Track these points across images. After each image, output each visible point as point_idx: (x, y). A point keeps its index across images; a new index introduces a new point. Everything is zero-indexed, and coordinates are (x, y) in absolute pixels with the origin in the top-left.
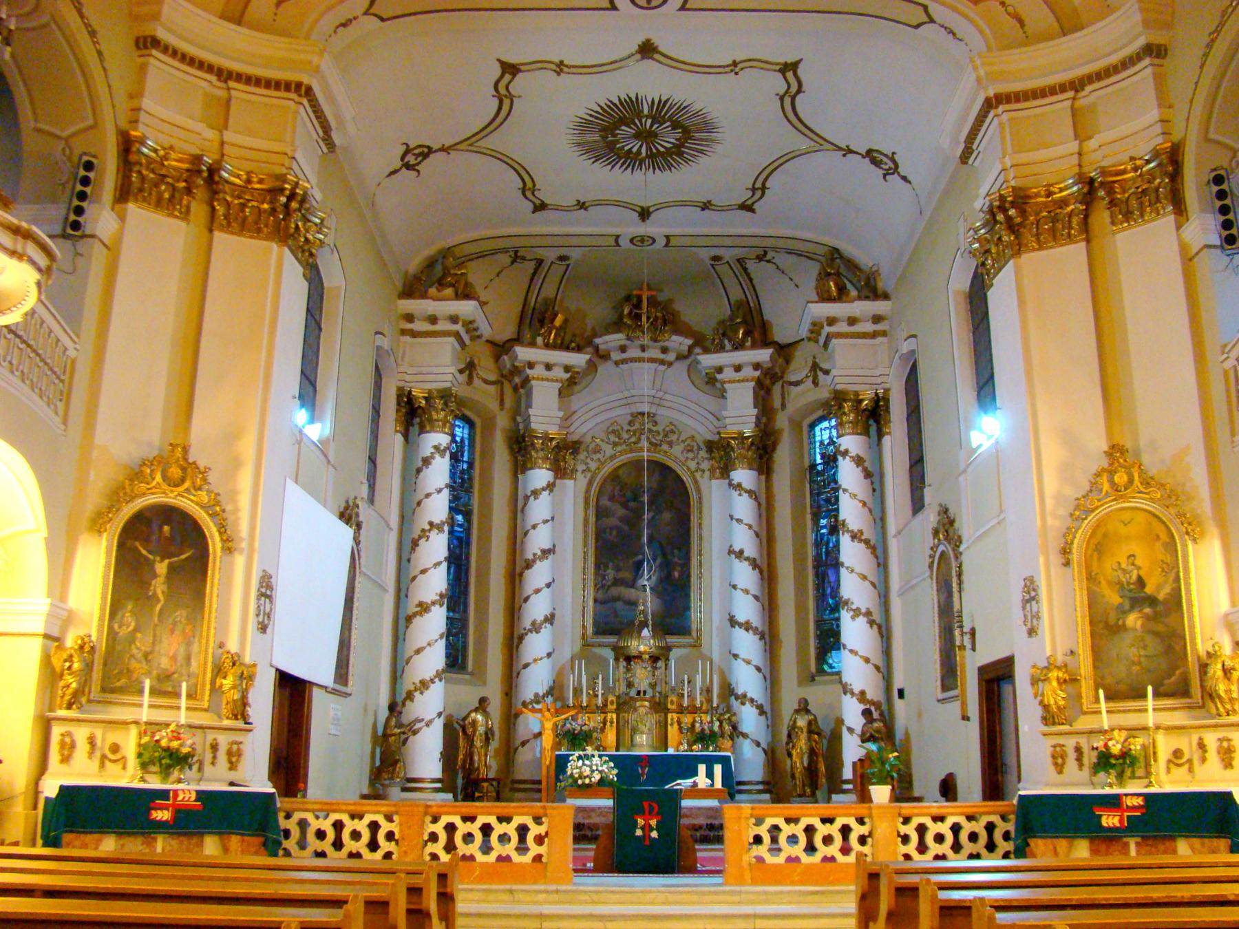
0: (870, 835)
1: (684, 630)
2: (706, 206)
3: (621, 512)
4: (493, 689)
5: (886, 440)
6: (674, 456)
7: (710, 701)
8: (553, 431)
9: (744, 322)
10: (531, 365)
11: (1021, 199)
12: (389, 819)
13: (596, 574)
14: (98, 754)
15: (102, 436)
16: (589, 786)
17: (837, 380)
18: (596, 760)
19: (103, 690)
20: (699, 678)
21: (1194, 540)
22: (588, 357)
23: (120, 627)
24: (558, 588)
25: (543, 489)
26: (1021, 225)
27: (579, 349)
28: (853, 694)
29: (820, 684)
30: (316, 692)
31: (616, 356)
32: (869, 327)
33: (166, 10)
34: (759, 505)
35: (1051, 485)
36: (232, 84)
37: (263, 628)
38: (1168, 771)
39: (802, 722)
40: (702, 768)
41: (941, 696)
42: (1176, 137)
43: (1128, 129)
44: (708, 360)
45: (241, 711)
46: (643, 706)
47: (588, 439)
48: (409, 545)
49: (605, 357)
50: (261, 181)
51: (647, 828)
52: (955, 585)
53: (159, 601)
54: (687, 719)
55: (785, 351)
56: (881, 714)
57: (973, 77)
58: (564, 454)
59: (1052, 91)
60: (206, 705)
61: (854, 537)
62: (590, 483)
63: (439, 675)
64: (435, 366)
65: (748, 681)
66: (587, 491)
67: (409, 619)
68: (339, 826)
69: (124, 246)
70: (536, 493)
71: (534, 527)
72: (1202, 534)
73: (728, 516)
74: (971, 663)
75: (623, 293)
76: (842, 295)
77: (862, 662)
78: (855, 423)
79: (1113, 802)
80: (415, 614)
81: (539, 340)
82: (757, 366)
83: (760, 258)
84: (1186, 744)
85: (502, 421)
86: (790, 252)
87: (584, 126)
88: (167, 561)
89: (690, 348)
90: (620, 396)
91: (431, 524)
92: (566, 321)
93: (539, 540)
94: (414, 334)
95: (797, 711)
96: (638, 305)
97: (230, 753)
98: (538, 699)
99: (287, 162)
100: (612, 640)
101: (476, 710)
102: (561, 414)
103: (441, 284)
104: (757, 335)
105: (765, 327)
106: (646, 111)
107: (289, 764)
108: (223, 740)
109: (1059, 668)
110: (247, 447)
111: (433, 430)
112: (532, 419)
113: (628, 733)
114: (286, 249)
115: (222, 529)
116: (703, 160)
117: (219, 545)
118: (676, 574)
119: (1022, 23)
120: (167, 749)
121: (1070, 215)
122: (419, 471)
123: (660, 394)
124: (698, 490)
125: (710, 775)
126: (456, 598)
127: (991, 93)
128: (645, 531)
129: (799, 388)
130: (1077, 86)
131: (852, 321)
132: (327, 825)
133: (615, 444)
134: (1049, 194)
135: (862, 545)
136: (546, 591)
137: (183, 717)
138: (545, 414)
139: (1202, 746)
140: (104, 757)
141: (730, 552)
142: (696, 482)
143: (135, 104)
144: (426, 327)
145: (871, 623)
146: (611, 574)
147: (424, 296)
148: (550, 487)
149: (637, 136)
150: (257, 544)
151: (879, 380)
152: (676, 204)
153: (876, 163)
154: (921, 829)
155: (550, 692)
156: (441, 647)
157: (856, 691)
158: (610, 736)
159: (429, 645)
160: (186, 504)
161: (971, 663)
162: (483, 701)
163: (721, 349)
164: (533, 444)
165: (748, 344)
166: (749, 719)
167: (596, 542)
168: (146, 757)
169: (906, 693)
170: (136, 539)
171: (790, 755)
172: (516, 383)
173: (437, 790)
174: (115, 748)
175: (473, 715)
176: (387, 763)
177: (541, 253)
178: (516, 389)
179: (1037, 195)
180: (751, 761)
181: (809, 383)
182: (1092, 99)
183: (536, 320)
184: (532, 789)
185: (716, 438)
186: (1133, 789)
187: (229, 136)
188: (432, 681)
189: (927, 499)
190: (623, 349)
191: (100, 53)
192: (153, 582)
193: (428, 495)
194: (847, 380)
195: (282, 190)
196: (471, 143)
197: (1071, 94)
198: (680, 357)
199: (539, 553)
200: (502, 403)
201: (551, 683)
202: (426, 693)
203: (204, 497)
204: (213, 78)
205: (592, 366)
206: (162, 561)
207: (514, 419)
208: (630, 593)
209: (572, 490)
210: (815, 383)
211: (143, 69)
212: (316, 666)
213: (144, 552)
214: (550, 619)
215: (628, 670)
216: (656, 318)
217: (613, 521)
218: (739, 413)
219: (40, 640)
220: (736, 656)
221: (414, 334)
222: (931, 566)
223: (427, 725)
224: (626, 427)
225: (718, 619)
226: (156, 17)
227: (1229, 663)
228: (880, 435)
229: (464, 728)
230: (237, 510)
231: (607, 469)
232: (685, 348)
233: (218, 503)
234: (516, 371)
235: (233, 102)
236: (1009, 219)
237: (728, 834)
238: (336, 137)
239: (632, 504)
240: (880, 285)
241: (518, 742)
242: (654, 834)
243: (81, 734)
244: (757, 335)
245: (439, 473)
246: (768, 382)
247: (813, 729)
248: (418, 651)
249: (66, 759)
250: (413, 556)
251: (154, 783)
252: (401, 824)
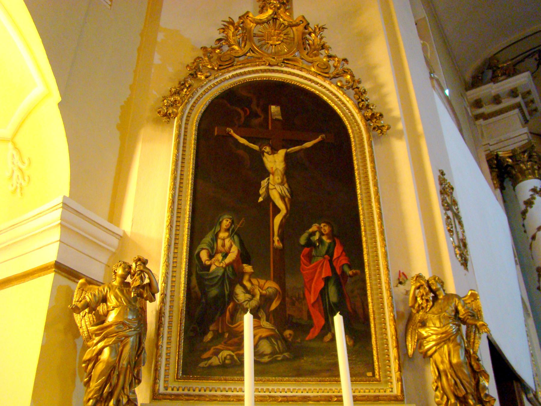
23: (211, 256)
37: (465, 262)
53: (277, 210)
60: (396, 391)
88: (282, 153)
111: (525, 177)
122: (524, 213)
150: (420, 128)
170: (229, 127)
192: (264, 183)
206: (274, 150)
213: (242, 141)
219: (49, 278)
221: (485, 117)
230: (379, 87)
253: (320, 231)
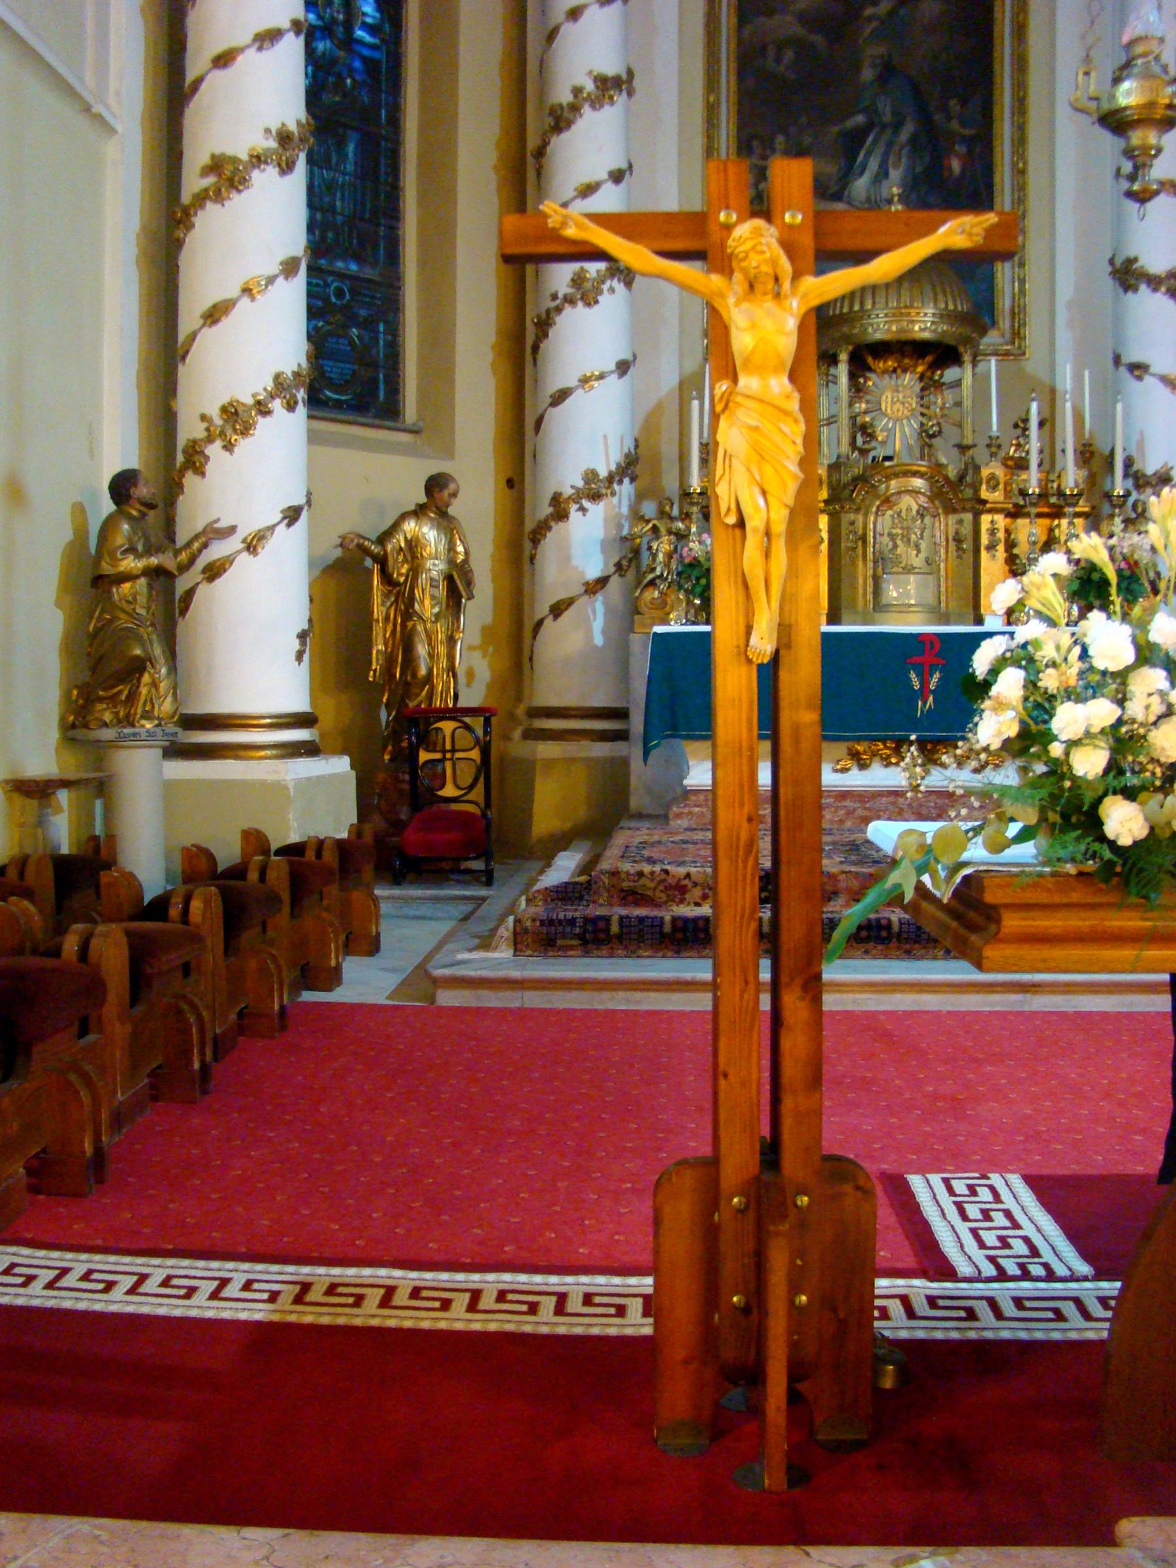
63: (281, 386)
80: (201, 199)
101: (419, 512)
118: (956, 165)
155: (628, 468)
159: (247, 291)
167: (741, 74)
175: (410, 526)
188: (262, 409)
199: (589, 86)
201: (629, 445)
202: (244, 445)
215: (857, 389)
223: (252, 546)
241: (543, 609)
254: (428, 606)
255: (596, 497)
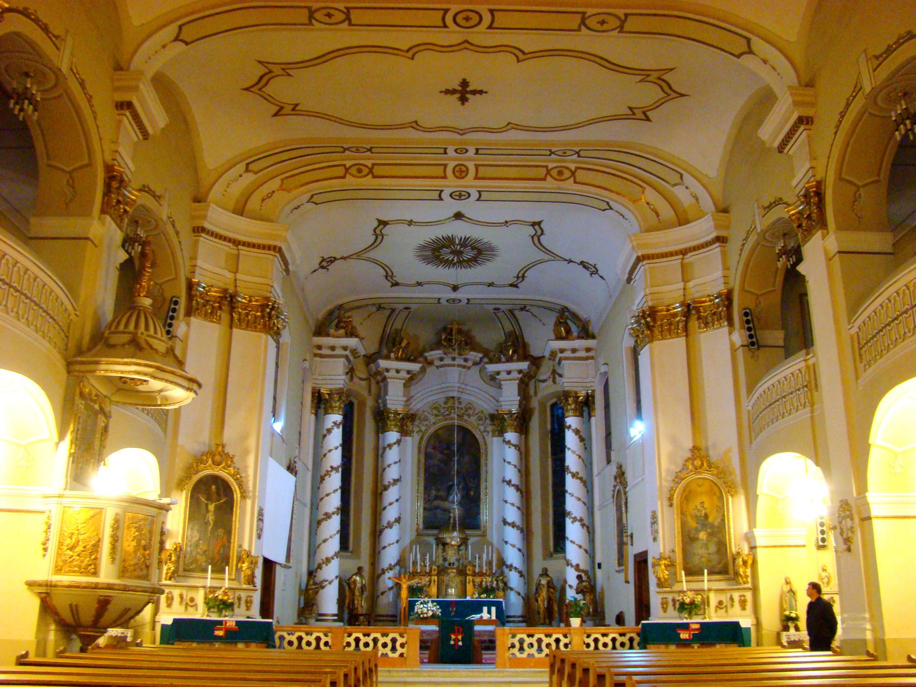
0: (570, 643)
1: (476, 526)
2: (491, 285)
3: (439, 456)
4: (364, 561)
5: (593, 419)
6: (472, 423)
7: (491, 569)
8: (400, 409)
9: (513, 344)
10: (388, 370)
11: (653, 312)
12: (326, 635)
13: (425, 493)
14: (184, 603)
15: (182, 440)
16: (427, 618)
17: (565, 385)
18: (430, 604)
19: (185, 570)
20: (485, 556)
21: (732, 496)
22: (420, 365)
24: (403, 503)
25: (395, 444)
26: (653, 326)
27: (414, 361)
28: (572, 566)
29: (556, 559)
30: (278, 567)
31: (437, 363)
32: (583, 354)
33: (209, 214)
34: (521, 453)
35: (665, 464)
36: (240, 247)
37: (259, 537)
38: (716, 611)
39: (544, 581)
40: (485, 609)
41: (617, 569)
42: (730, 286)
43: (710, 278)
44: (492, 368)
45: (251, 580)
46: (453, 572)
47: (421, 412)
48: (319, 479)
49: (430, 363)
50: (256, 301)
51: (456, 640)
52: (624, 509)
54: (478, 580)
55: (536, 362)
56: (588, 578)
57: (630, 246)
58: (406, 422)
59: (671, 254)
61: (574, 475)
62: (422, 438)
63: (336, 554)
64: (334, 376)
65: (513, 557)
66: (420, 443)
67: (319, 523)
68: (300, 639)
69: (190, 341)
70: (390, 446)
71: (389, 466)
72: (736, 492)
73: (502, 459)
74: (632, 551)
75: (440, 326)
76: (568, 336)
77: (577, 547)
78: (575, 410)
79: (685, 627)
81: (392, 355)
82: (520, 372)
83: (522, 309)
84: (724, 598)
85: (370, 402)
86: (539, 307)
87: (423, 248)
89: (481, 359)
90: (439, 387)
91: (332, 467)
92: (408, 343)
93: (392, 473)
94: (321, 356)
95: (541, 575)
96: (450, 333)
97: (247, 602)
98: (391, 568)
99: (269, 289)
100: (435, 532)
101: (356, 574)
102: (405, 399)
103: (338, 327)
104: (520, 351)
105: (525, 346)
106: (457, 242)
107: (267, 608)
108: (243, 595)
109: (665, 559)
110: (252, 442)
112: (388, 402)
113: (444, 587)
114: (270, 337)
115: (240, 486)
116: (488, 264)
117: (239, 495)
119: (658, 215)
120: (222, 600)
121: (678, 322)
122: (324, 436)
123: (463, 386)
124: (486, 444)
125: (489, 612)
126: (344, 510)
127: (640, 254)
128: (452, 467)
129: (545, 384)
130: (684, 252)
131: (574, 351)
132: (293, 638)
133: (436, 415)
134: (668, 310)
135: (578, 481)
136: (396, 504)
137: (227, 584)
138: (395, 399)
139: (732, 599)
140: (187, 604)
141: (504, 481)
142: (484, 438)
143: (193, 263)
144: (329, 352)
145: (583, 525)
146: (434, 493)
147: (328, 335)
148: (398, 442)
149: (452, 252)
151: (589, 385)
152: (473, 284)
153: (585, 267)
154: (596, 640)
155: (398, 563)
156: (337, 538)
157: (574, 563)
158: (434, 590)
160: (224, 474)
161: (632, 551)
162: (360, 569)
163: (499, 361)
164: (388, 417)
165: (515, 358)
166: (514, 579)
168: (211, 604)
169: (602, 566)
171: (537, 601)
172: (379, 380)
173: (335, 621)
174: (192, 600)
176: (308, 606)
177: (394, 306)
178: (378, 383)
179: (662, 311)
180: (515, 604)
181: (550, 382)
182: (691, 259)
183: (391, 343)
184: (393, 619)
185: (496, 413)
186: (695, 621)
187: (239, 276)
188: (333, 558)
189: (613, 458)
190: (441, 359)
191: (180, 242)
193: (330, 451)
194: (570, 384)
195: (268, 306)
196: (358, 255)
197: (681, 256)
198: (475, 364)
200: (370, 391)
202: (329, 565)
203: (232, 470)
204: (231, 245)
205: (423, 370)
207: (377, 400)
208: (446, 504)
209: (410, 442)
210: (554, 382)
211: (197, 242)
212: (278, 555)
214: (398, 520)
215: (444, 551)
216: (461, 341)
217: (436, 462)
218: (509, 399)
220: (506, 542)
221: (321, 356)
222: (613, 496)
223: (330, 583)
224: (443, 405)
225: (496, 520)
226: (205, 217)
227: (746, 558)
228: (590, 416)
229: (349, 585)
230: (247, 476)
231: (432, 430)
232: (478, 359)
233: (238, 474)
234: (378, 373)
235: (241, 258)
236: (647, 323)
237: (498, 643)
238: (291, 268)
239: (446, 452)
240: (590, 328)
241: (379, 593)
242: (460, 643)
243: (176, 593)
244: (520, 351)
245: (336, 438)
246: (526, 380)
247: (550, 585)
248: (325, 541)
249: (169, 606)
250: (321, 486)
251: (214, 617)
252: (332, 638)
253: (221, 531)
254: (357, 593)
255: (391, 569)
